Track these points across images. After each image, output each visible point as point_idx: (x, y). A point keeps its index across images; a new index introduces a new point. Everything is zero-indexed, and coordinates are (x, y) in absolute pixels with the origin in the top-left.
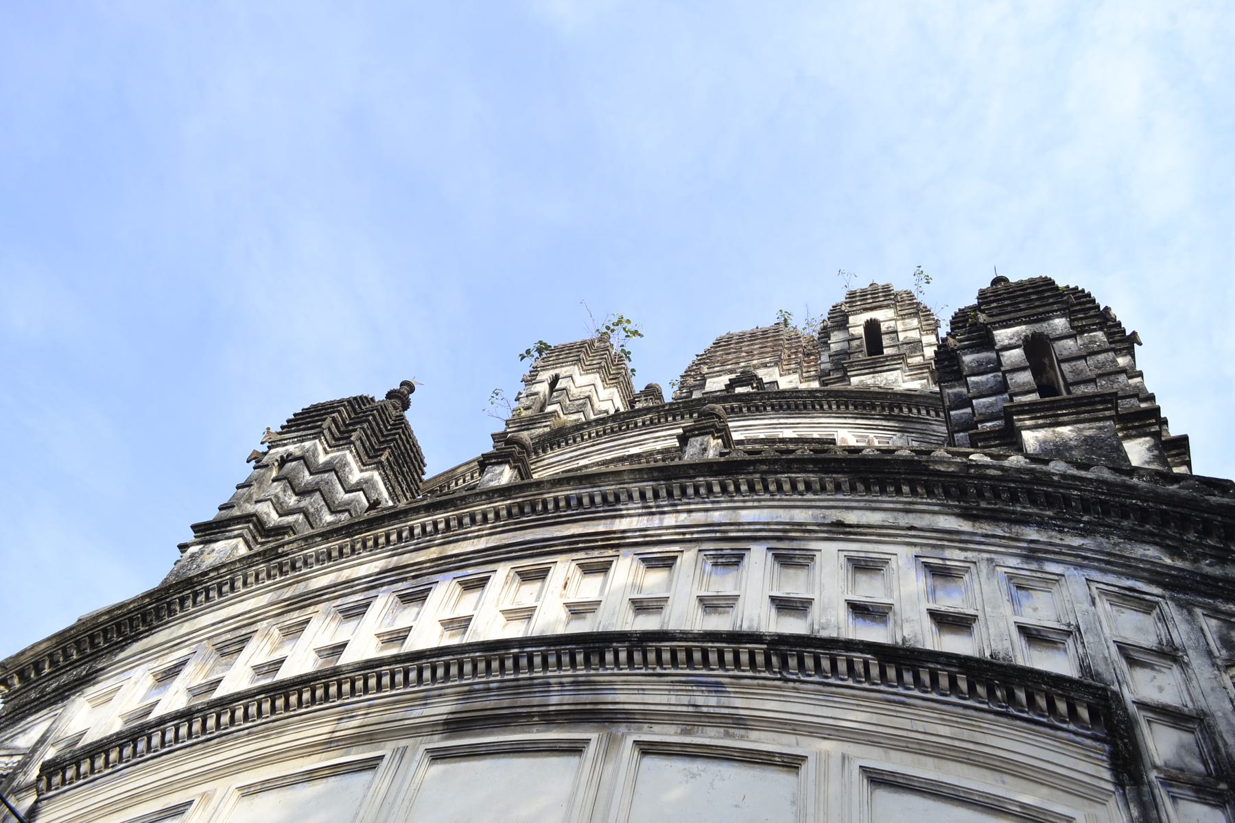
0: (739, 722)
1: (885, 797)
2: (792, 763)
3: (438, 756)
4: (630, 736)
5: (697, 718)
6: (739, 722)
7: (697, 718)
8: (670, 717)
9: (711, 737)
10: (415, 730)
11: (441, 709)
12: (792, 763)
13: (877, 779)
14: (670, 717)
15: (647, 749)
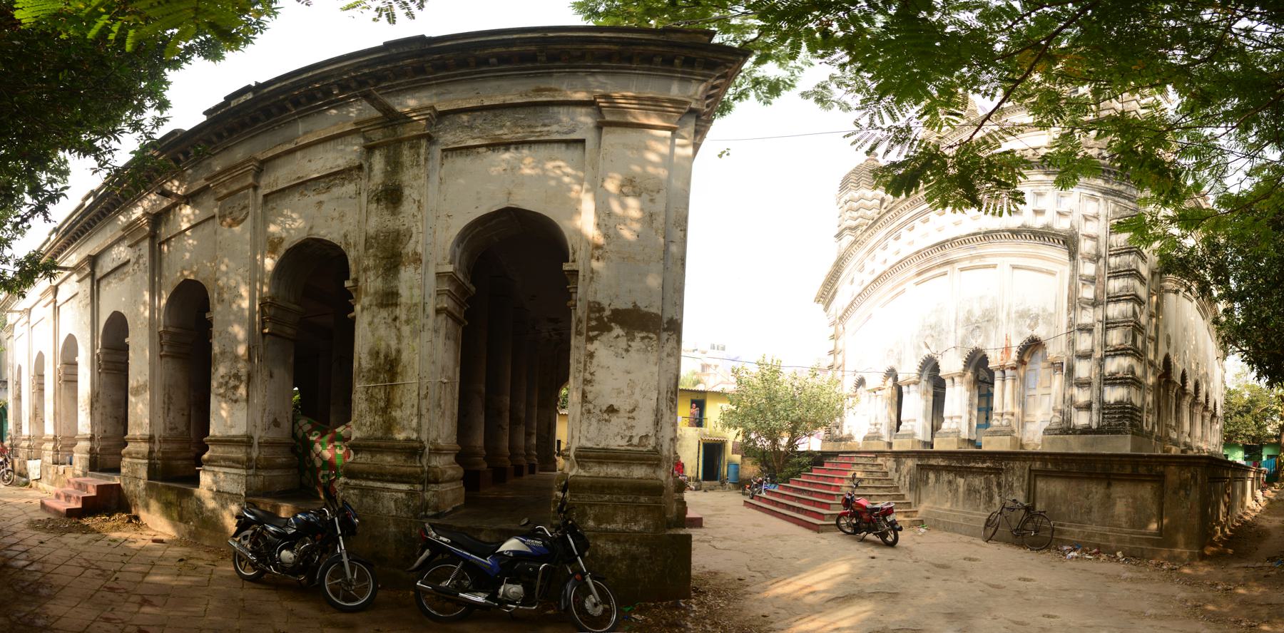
0: (982, 256)
1: (1016, 271)
2: (995, 266)
3: (917, 284)
4: (957, 266)
5: (972, 258)
6: (982, 256)
7: (972, 258)
8: (966, 259)
9: (977, 262)
10: (910, 279)
11: (914, 270)
12: (995, 266)
13: (1014, 267)
14: (966, 259)
15: (962, 270)
